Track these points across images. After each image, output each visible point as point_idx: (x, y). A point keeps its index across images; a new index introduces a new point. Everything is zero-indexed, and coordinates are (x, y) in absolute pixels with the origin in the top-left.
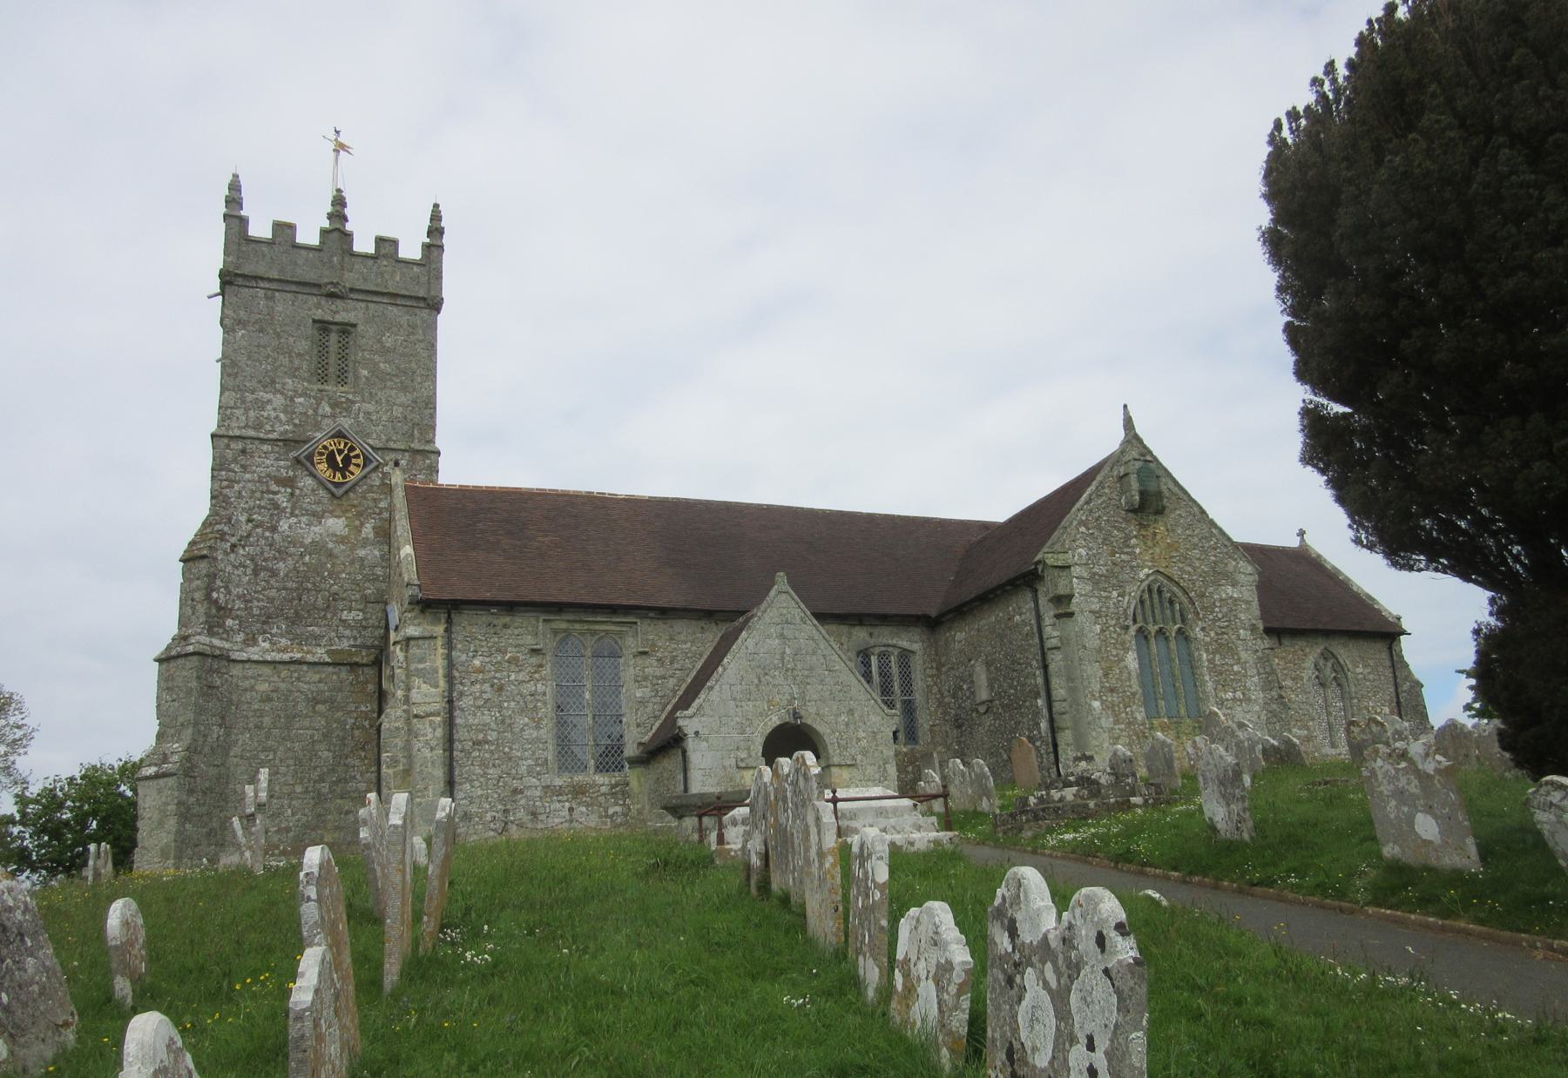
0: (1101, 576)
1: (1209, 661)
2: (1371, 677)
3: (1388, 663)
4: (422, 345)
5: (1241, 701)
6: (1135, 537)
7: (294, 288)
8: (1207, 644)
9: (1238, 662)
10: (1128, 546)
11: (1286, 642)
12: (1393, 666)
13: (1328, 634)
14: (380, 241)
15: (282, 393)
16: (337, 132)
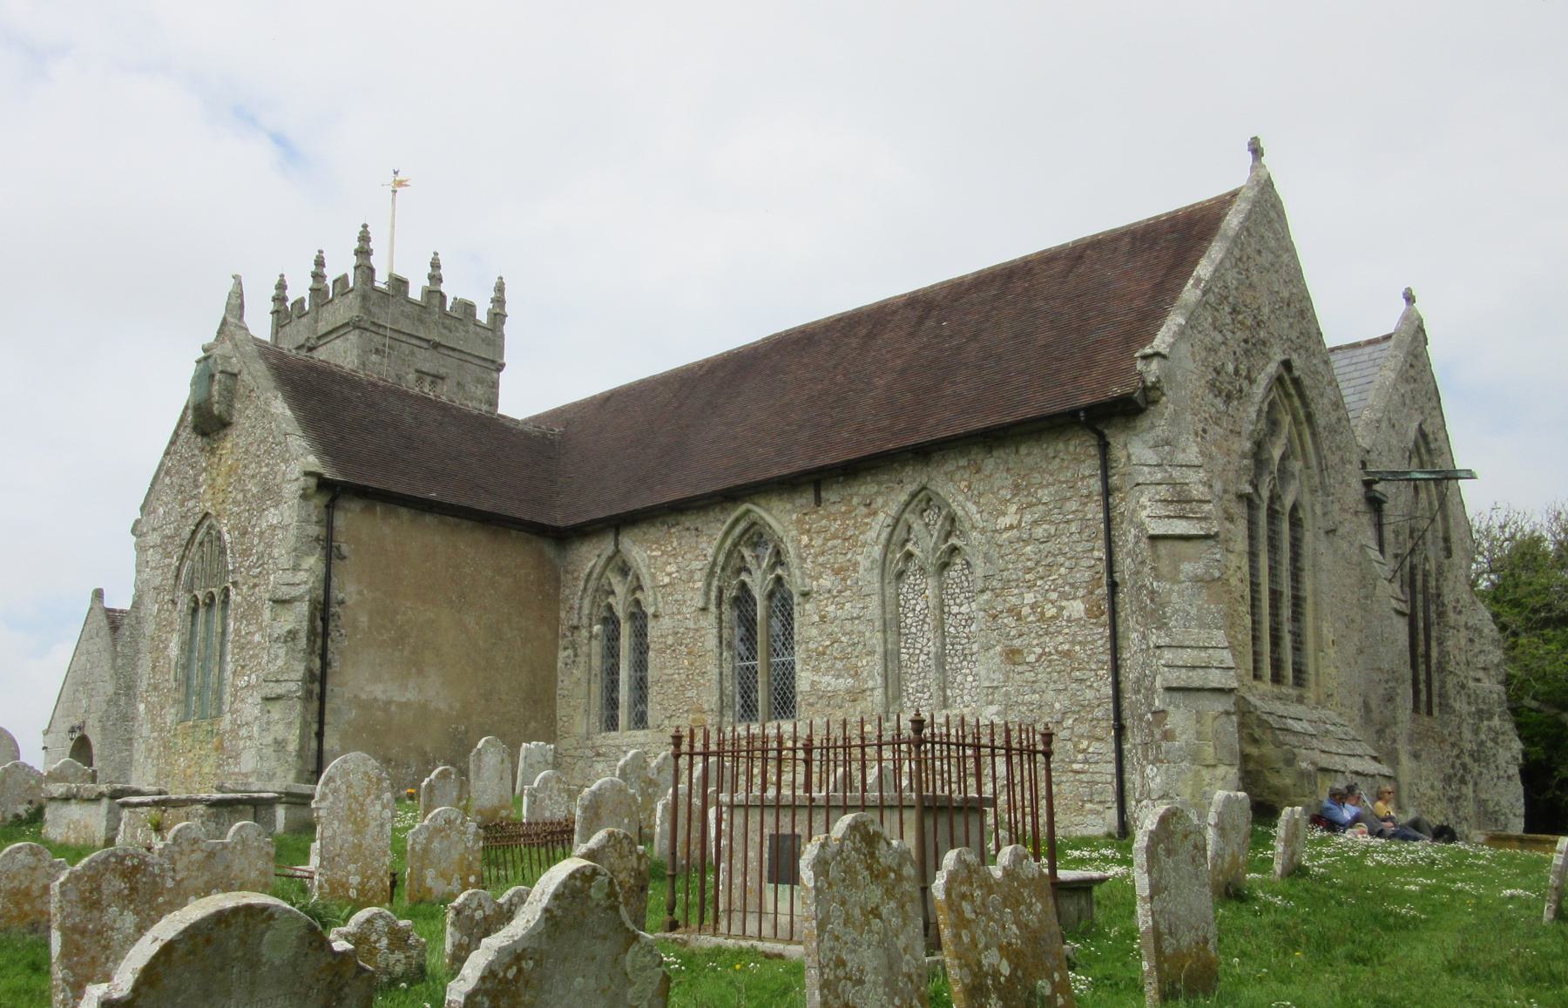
0: (169, 537)
2: (1039, 532)
3: (1096, 485)
6: (205, 470)
8: (239, 605)
11: (830, 495)
12: (1107, 492)
13: (924, 453)
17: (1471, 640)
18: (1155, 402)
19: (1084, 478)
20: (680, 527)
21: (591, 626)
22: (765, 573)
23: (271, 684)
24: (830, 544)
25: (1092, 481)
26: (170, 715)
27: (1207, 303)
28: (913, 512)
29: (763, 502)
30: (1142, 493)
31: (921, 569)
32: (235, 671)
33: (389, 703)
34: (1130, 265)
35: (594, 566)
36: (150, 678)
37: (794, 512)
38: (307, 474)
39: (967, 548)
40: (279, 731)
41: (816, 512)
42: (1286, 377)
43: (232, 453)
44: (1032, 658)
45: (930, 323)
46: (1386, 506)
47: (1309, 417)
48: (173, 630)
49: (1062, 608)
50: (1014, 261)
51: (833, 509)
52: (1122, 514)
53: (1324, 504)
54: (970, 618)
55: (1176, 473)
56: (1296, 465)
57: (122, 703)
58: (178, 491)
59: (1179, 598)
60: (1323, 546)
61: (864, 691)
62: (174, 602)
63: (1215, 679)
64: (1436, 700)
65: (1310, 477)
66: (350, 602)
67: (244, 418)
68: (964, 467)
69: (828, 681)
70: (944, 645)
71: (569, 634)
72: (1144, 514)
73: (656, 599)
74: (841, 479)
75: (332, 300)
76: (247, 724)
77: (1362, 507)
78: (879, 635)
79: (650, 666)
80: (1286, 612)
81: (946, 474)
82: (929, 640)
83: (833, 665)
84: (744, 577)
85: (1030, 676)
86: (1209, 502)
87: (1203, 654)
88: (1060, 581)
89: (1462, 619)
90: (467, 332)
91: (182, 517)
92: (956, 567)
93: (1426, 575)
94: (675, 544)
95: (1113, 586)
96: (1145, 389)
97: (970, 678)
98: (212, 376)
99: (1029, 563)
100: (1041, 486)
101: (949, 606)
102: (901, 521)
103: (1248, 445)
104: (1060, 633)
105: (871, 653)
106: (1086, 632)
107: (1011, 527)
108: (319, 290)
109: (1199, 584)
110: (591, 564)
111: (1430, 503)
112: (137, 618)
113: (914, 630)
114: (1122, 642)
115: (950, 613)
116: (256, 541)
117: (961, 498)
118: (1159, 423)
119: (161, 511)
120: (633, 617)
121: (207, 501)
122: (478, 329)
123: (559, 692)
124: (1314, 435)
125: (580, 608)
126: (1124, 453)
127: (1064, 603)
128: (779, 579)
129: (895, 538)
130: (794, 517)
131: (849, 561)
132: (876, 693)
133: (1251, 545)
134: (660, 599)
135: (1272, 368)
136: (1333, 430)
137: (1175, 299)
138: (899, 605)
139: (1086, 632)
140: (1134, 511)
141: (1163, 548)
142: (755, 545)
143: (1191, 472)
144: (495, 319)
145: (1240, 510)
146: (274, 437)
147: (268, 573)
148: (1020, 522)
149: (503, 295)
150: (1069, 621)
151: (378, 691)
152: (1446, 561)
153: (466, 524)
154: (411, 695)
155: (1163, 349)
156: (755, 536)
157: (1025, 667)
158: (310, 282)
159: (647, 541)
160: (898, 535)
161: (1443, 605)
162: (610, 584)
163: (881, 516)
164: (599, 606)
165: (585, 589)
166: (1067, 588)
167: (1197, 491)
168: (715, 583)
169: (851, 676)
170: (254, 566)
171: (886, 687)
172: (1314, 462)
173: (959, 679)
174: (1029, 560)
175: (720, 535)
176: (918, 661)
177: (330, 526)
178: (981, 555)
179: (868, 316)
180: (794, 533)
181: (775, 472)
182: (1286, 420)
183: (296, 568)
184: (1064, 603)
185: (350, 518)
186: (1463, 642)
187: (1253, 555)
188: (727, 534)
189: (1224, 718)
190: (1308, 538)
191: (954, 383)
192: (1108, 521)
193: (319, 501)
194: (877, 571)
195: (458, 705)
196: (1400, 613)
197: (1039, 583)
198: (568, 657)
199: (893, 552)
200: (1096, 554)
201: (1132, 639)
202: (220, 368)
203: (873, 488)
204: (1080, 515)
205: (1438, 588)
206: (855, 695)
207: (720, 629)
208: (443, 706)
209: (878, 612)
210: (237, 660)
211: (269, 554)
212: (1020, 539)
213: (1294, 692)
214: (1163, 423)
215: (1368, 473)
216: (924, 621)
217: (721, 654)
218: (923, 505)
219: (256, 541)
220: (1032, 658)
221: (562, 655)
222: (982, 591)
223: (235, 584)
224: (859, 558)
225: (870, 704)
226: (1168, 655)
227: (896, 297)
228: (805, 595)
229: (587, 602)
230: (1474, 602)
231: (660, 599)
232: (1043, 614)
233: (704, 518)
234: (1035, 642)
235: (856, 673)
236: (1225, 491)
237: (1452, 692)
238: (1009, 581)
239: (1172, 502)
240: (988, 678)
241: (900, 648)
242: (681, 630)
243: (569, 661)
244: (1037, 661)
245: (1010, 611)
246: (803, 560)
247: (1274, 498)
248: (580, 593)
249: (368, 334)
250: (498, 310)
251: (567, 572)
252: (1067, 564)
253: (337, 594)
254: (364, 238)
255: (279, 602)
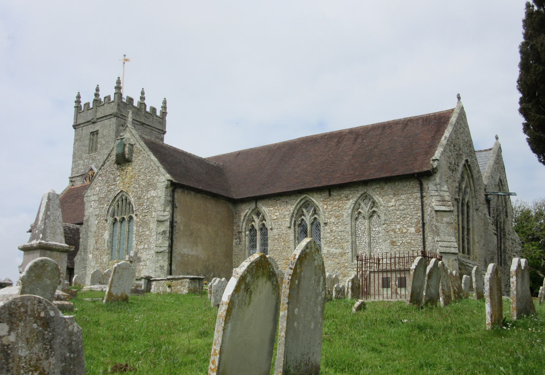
0: (102, 198)
1: (136, 230)
2: (401, 208)
3: (419, 195)
4: (112, 131)
5: (146, 249)
6: (119, 176)
7: (87, 124)
8: (138, 222)
9: (149, 229)
10: (115, 181)
11: (334, 193)
12: (422, 197)
13: (366, 183)
14: (105, 98)
15: (83, 160)
16: (125, 56)
17: (513, 244)
18: (436, 173)
19: (415, 193)
20: (281, 201)
21: (246, 232)
22: (311, 216)
23: (158, 248)
24: (334, 208)
25: (417, 194)
26: (105, 259)
27: (448, 144)
28: (361, 200)
29: (310, 194)
30: (433, 198)
31: (363, 217)
32: (137, 244)
33: (188, 255)
34: (423, 129)
35: (247, 212)
36: (94, 246)
37: (322, 198)
38: (168, 180)
39: (379, 212)
40: (161, 263)
41: (329, 198)
42: (466, 164)
43: (132, 171)
44: (399, 244)
45: (359, 140)
46: (491, 202)
47: (472, 176)
48: (106, 230)
49: (408, 230)
50: (385, 122)
51: (335, 198)
52: (426, 204)
53: (475, 202)
54: (379, 232)
55: (441, 193)
56: (468, 190)
57: (82, 254)
58: (106, 182)
59: (442, 228)
60: (475, 214)
61: (345, 253)
62: (106, 220)
63: (453, 250)
64: (503, 261)
65: (472, 193)
66: (178, 222)
67: (137, 160)
68: (378, 188)
69: (333, 250)
70: (370, 240)
71: (237, 234)
72: (433, 204)
73: (271, 224)
74: (338, 189)
75: (103, 105)
76: (143, 261)
77: (484, 202)
78: (350, 237)
79: (269, 245)
80: (466, 233)
81: (373, 189)
82: (366, 238)
83: (335, 245)
84: (303, 217)
85: (398, 249)
86: (450, 201)
87: (449, 243)
88: (408, 222)
89: (510, 237)
90: (153, 119)
91: (108, 191)
92: (375, 217)
93: (501, 223)
94: (278, 206)
95: (424, 224)
96: (433, 169)
97: (379, 250)
98: (125, 145)
99: (398, 217)
100: (402, 194)
101: (372, 228)
102: (358, 202)
103: (458, 185)
104: (407, 237)
105: (348, 242)
106: (415, 237)
107: (393, 206)
108: (98, 100)
109: (448, 224)
110: (246, 211)
111: (502, 201)
112: (87, 225)
113: (361, 235)
114: (426, 240)
115: (372, 230)
116: (146, 201)
117: (377, 196)
118: (437, 178)
119: (98, 189)
120: (261, 229)
121: (121, 186)
122: (157, 118)
123: (234, 253)
124: (473, 181)
125: (242, 226)
126: (427, 186)
127: (409, 228)
128: (315, 218)
129: (355, 207)
130: (322, 199)
131: (340, 214)
132: (349, 254)
133: (458, 213)
134: (273, 223)
135: (463, 162)
136: (478, 180)
137: (439, 142)
138: (356, 228)
139: (415, 237)
140: (430, 203)
141: (439, 214)
142: (306, 208)
143: (445, 193)
144: (163, 114)
145: (455, 203)
146: (152, 167)
147: (151, 212)
148: (395, 204)
149: (166, 105)
150: (410, 233)
151: (186, 251)
152: (506, 219)
153: (209, 197)
154: (194, 253)
155: (438, 159)
156: (307, 204)
157: (397, 247)
158: (93, 97)
159: (268, 205)
160: (356, 207)
161: (505, 232)
162: (253, 218)
163: (351, 201)
164: (248, 225)
165: (244, 220)
166: (410, 224)
167: (447, 198)
168: (293, 219)
169: (341, 249)
170: (145, 209)
171: (352, 252)
172: (473, 189)
173: (375, 250)
174: (398, 216)
175: (296, 204)
176: (362, 245)
177: (173, 196)
178: (383, 214)
179: (336, 135)
180: (322, 204)
181: (316, 185)
182: (466, 177)
183: (164, 211)
184: (409, 228)
185: (178, 194)
186: (510, 244)
187: (458, 216)
188: (298, 203)
189: (455, 261)
190: (471, 211)
191: (372, 161)
192: (422, 205)
193: (170, 189)
194: (350, 217)
195: (206, 257)
196: (495, 234)
197: (401, 222)
198: (237, 242)
199: (355, 212)
200: (418, 215)
201: (429, 239)
202: (128, 143)
203: (349, 192)
204: (414, 203)
205: (503, 227)
206: (342, 255)
207: (295, 233)
208: (203, 257)
209: (350, 229)
210: (138, 240)
211: (152, 206)
212: (395, 209)
213: (467, 256)
214: (438, 179)
215: (486, 192)
216: (364, 232)
217: (295, 242)
218: (364, 198)
219: (146, 201)
220: (399, 244)
221: (235, 241)
222: (384, 224)
223: (136, 215)
224: (344, 213)
225: (347, 257)
226: (440, 243)
227: (345, 130)
228: (326, 224)
229: (244, 223)
230: (513, 232)
231: (273, 223)
232: (402, 231)
233: (289, 198)
234: (400, 239)
235: (343, 248)
236: (452, 198)
237: (507, 259)
238: (392, 221)
239: (441, 201)
240: (385, 250)
241: (356, 240)
242: (281, 234)
243: (237, 243)
244: (400, 245)
245: (392, 230)
246: (325, 213)
247: (463, 199)
248: (242, 221)
249: (119, 119)
250: (164, 111)
251: (236, 213)
252: (410, 217)
253: (175, 220)
254: (119, 82)
255: (160, 222)
